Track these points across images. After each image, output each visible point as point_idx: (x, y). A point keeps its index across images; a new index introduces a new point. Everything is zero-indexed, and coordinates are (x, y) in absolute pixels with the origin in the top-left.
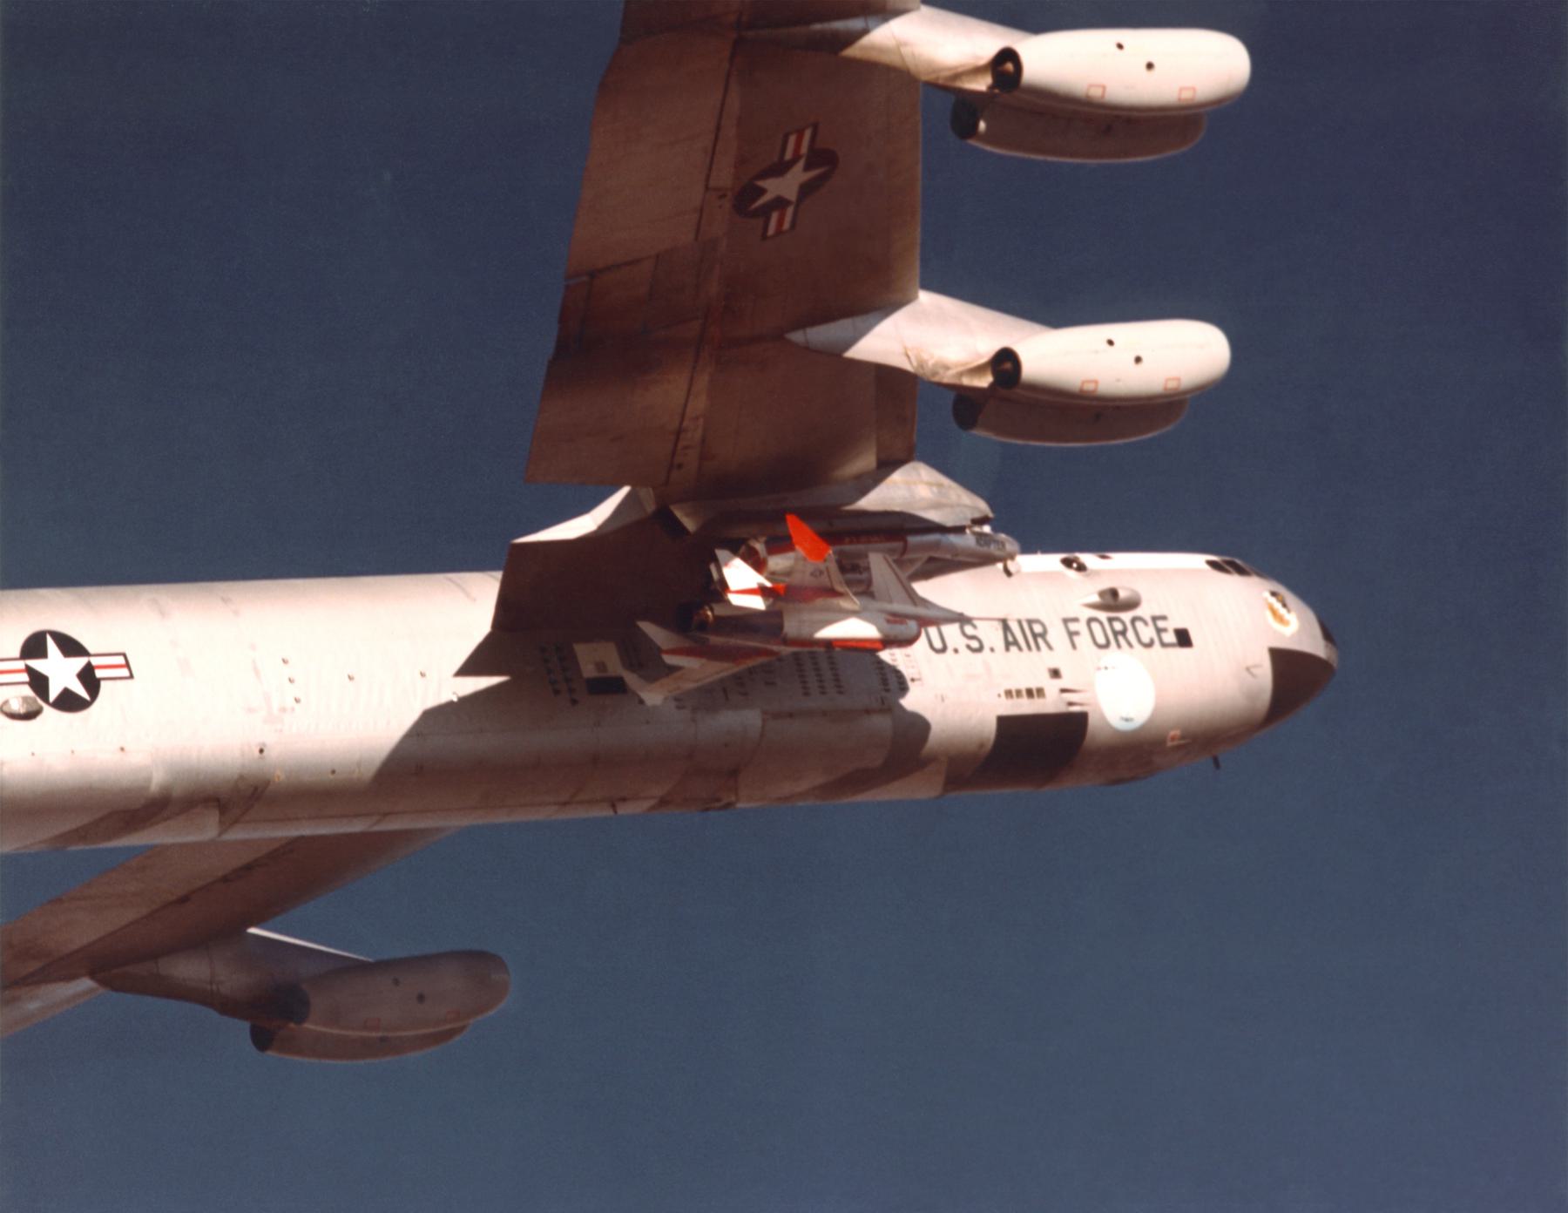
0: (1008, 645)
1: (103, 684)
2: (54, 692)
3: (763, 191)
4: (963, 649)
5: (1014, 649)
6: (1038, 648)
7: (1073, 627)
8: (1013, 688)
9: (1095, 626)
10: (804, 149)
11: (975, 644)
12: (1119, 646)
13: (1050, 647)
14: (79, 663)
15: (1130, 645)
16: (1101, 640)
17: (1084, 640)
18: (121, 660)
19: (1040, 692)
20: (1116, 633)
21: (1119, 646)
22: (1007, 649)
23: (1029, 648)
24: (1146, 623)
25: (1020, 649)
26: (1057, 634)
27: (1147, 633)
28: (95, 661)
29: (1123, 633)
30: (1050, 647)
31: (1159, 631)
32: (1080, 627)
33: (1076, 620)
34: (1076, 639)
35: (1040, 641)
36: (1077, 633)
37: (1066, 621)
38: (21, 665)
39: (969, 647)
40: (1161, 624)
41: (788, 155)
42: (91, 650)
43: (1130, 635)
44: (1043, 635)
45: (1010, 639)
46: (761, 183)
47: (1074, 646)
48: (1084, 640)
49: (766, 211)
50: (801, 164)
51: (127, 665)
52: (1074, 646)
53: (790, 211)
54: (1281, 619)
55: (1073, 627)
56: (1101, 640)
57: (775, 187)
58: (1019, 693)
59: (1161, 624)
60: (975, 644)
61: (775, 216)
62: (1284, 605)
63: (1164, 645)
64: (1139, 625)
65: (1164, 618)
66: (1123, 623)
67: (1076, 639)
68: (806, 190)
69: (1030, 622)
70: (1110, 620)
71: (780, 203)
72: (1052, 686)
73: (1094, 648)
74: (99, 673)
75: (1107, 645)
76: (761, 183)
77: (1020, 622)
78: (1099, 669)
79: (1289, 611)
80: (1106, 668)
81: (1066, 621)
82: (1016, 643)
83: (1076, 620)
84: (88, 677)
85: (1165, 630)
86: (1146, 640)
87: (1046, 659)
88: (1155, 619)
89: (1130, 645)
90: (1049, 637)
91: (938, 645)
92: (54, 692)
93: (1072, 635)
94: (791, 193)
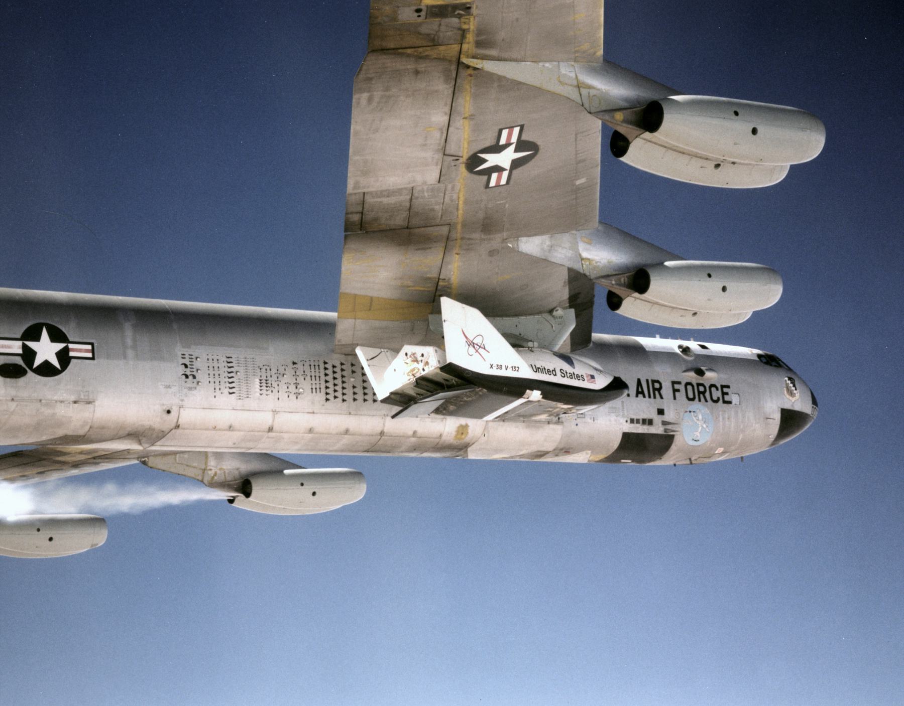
0: (638, 393)
1: (73, 361)
2: (38, 362)
3: (485, 161)
5: (640, 396)
6: (655, 397)
7: (677, 386)
8: (635, 417)
9: (689, 387)
10: (514, 139)
12: (700, 400)
14: (60, 346)
15: (706, 401)
16: (691, 396)
17: (681, 396)
18: (89, 347)
19: (650, 422)
20: (699, 393)
21: (700, 400)
22: (637, 396)
23: (650, 397)
24: (717, 389)
25: (644, 396)
26: (667, 390)
27: (717, 394)
28: (71, 346)
29: (704, 393)
30: (662, 398)
31: (724, 394)
32: (681, 387)
33: (679, 383)
34: (677, 394)
35: (657, 393)
36: (678, 390)
37: (673, 383)
38: (20, 343)
40: (725, 390)
41: (503, 141)
42: (71, 339)
43: (707, 394)
44: (659, 390)
45: (640, 390)
46: (483, 156)
47: (675, 398)
48: (681, 396)
49: (489, 172)
50: (513, 147)
51: (93, 351)
52: (675, 398)
53: (505, 174)
54: (791, 394)
55: (677, 386)
56: (691, 396)
57: (492, 160)
58: (638, 421)
59: (725, 390)
61: (494, 176)
62: (794, 386)
63: (725, 402)
64: (713, 389)
65: (728, 387)
66: (705, 387)
67: (677, 394)
68: (516, 164)
69: (654, 382)
71: (498, 169)
72: (657, 419)
73: (687, 401)
74: (71, 354)
75: (693, 399)
76: (483, 156)
77: (647, 381)
78: (686, 412)
79: (796, 389)
80: (690, 412)
81: (673, 383)
82: (642, 393)
83: (679, 383)
84: (64, 357)
85: (727, 394)
86: (715, 398)
87: (657, 403)
88: (723, 387)
89: (706, 401)
90: (661, 392)
92: (38, 362)
93: (675, 391)
94: (507, 165)
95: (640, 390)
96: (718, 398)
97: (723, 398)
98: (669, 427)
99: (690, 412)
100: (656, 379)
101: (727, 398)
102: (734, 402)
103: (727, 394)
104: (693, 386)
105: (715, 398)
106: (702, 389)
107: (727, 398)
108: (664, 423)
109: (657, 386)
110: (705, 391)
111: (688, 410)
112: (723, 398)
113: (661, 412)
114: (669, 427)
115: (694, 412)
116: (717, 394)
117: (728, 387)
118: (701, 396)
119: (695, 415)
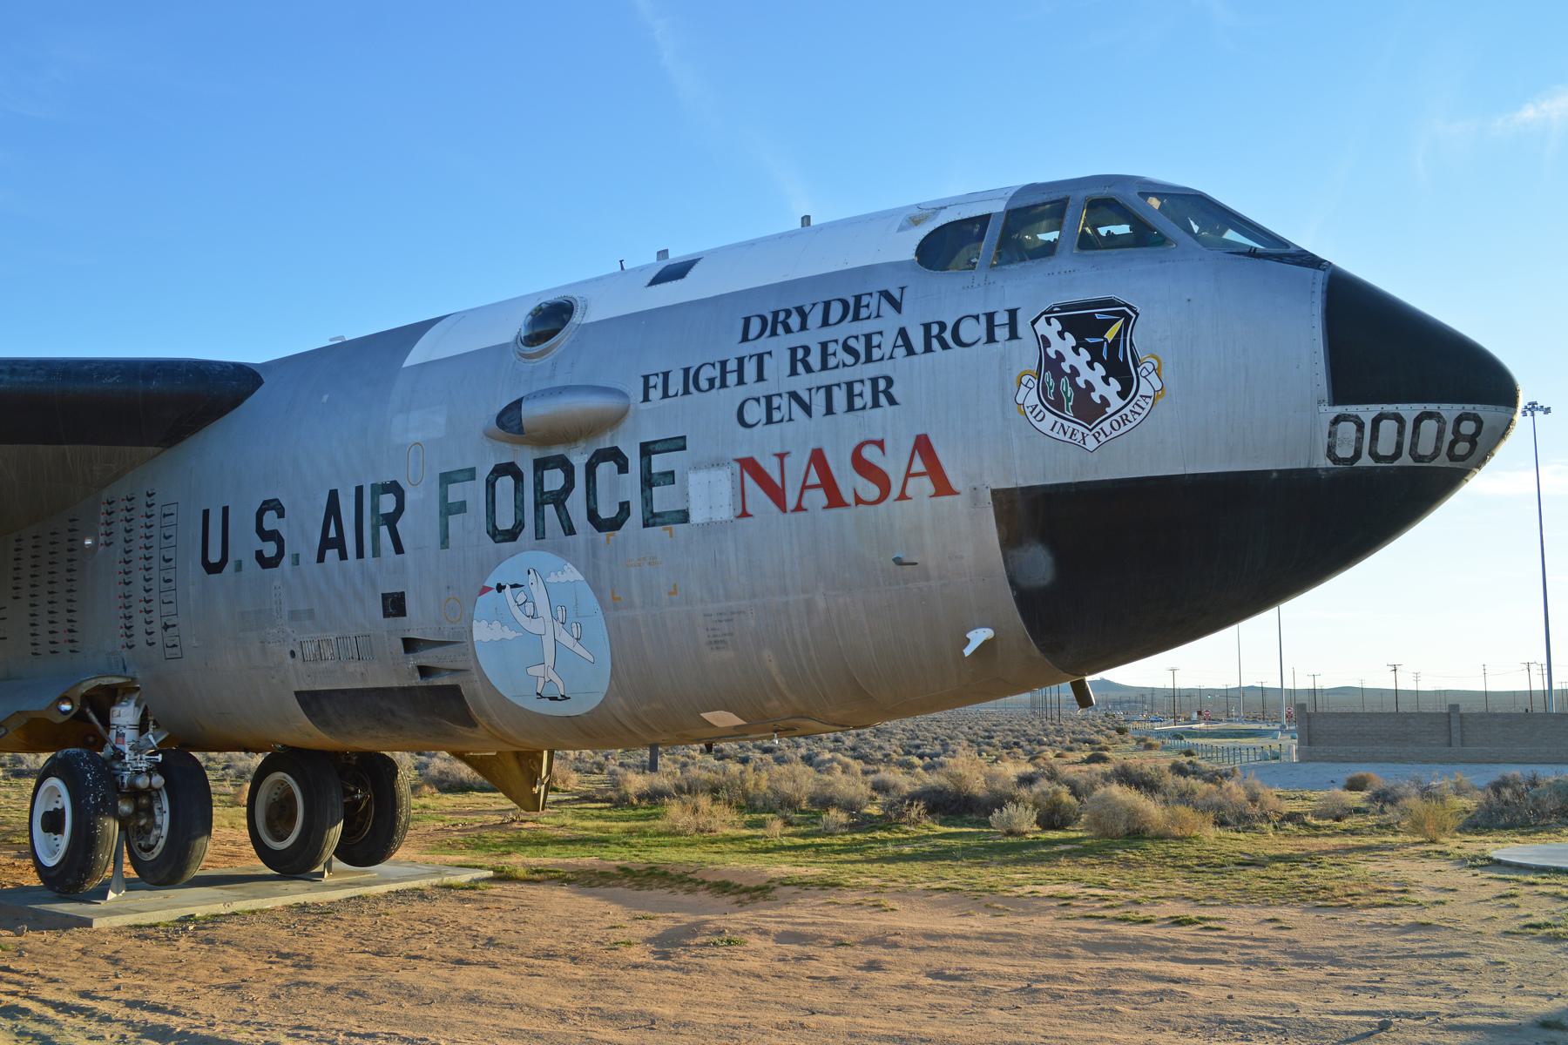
0: (326, 543)
4: (251, 564)
5: (332, 554)
6: (376, 552)
7: (456, 493)
11: (270, 549)
12: (540, 534)
13: (399, 549)
21: (540, 534)
22: (321, 559)
23: (360, 554)
24: (623, 468)
25: (343, 556)
29: (559, 499)
30: (399, 549)
31: (648, 481)
32: (472, 493)
33: (471, 474)
35: (384, 530)
36: (461, 507)
37: (447, 479)
39: (259, 555)
40: (659, 463)
43: (576, 504)
44: (391, 520)
45: (332, 534)
47: (444, 542)
52: (444, 542)
55: (456, 493)
59: (659, 463)
60: (270, 549)
63: (651, 519)
64: (605, 469)
65: (678, 444)
70: (541, 465)
75: (512, 535)
77: (359, 490)
78: (485, 590)
82: (339, 543)
83: (471, 474)
85: (669, 477)
86: (606, 511)
87: (386, 572)
88: (647, 450)
89: (570, 530)
91: (214, 557)
93: (450, 509)
95: (332, 534)
96: (625, 508)
97: (647, 501)
98: (427, 657)
99: (500, 588)
100: (387, 478)
101: (663, 498)
102: (695, 518)
103: (669, 477)
104: (518, 476)
105: (606, 511)
106: (554, 480)
107: (663, 498)
108: (410, 645)
109: (388, 503)
110: (569, 484)
111: (491, 582)
112: (647, 501)
113: (395, 605)
114: (427, 657)
115: (514, 586)
116: (618, 488)
117: (678, 444)
118: (550, 509)
119: (521, 598)
